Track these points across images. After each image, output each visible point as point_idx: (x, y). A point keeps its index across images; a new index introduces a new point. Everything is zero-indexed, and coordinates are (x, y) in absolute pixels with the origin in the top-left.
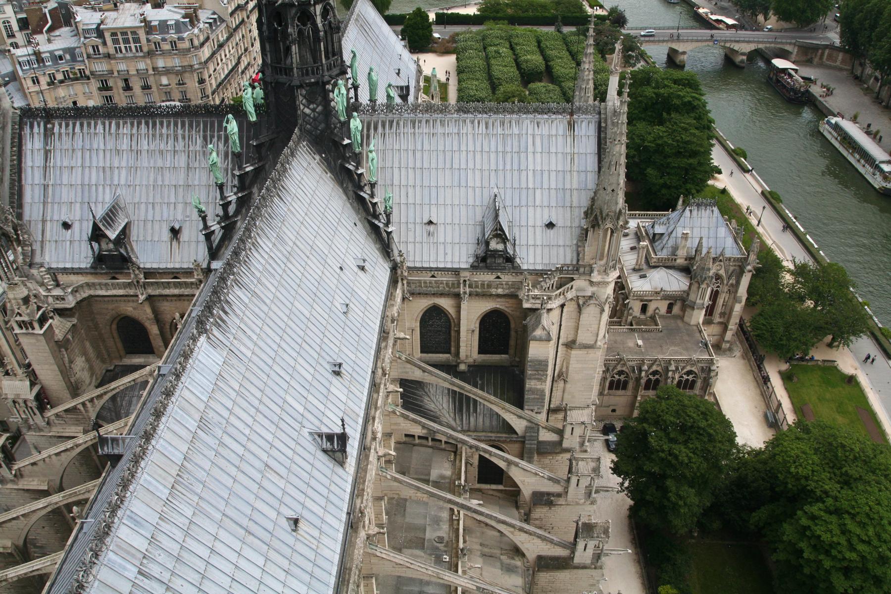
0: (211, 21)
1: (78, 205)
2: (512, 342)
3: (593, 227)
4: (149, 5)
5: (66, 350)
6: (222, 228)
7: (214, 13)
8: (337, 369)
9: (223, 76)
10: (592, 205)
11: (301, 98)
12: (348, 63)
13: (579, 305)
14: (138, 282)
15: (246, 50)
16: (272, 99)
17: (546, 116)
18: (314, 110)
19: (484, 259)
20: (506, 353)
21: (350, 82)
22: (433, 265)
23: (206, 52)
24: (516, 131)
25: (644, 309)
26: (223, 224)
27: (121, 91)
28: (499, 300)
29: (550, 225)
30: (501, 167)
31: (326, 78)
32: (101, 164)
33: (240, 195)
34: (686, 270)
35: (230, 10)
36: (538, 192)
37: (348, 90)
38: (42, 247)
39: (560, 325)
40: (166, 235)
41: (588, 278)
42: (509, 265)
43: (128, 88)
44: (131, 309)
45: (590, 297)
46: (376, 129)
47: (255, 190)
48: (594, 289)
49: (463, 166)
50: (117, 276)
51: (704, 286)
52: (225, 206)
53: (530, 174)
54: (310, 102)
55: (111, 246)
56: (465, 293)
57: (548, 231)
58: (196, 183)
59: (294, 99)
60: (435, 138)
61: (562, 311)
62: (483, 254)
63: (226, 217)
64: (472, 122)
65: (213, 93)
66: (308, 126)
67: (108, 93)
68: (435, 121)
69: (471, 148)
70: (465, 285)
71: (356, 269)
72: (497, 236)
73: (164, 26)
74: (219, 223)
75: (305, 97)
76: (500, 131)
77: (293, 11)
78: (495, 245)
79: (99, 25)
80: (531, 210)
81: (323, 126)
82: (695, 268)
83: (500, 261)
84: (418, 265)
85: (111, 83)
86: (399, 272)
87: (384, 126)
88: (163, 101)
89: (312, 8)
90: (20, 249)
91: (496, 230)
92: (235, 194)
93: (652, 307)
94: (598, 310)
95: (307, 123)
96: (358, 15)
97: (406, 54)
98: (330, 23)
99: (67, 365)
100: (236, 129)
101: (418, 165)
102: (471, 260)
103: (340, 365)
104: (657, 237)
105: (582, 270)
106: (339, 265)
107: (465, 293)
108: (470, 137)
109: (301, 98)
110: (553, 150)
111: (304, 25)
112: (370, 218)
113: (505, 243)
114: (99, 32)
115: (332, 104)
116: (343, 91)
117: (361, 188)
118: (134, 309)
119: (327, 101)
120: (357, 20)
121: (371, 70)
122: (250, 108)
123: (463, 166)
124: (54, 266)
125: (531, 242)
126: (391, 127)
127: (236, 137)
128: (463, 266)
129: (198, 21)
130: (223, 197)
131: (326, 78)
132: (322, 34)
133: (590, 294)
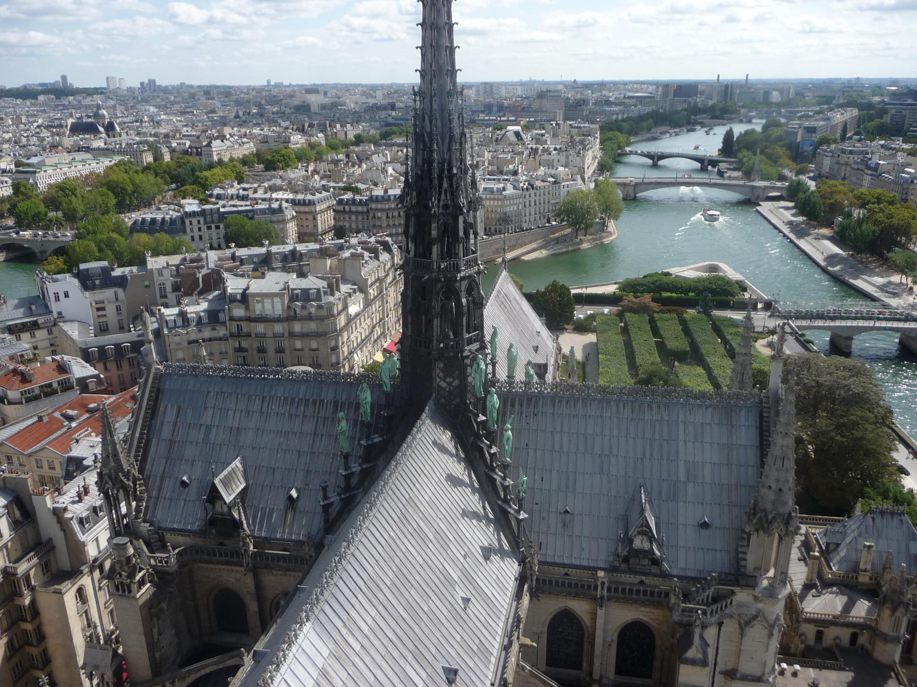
1: (200, 463)
2: (657, 664)
3: (757, 530)
4: (295, 276)
5: (159, 619)
6: (342, 500)
7: (354, 284)
8: (451, 677)
10: (756, 505)
11: (438, 371)
12: (488, 338)
13: (740, 625)
14: (245, 551)
18: (450, 384)
19: (626, 560)
20: (650, 677)
21: (489, 357)
22: (566, 561)
24: (666, 418)
25: (819, 636)
26: (343, 496)
27: (255, 352)
28: (642, 609)
29: (705, 525)
30: (648, 456)
31: (466, 353)
32: (229, 424)
33: (364, 466)
34: (872, 592)
35: (369, 282)
36: (690, 487)
37: (487, 365)
38: (156, 504)
39: (717, 648)
40: (281, 502)
41: (751, 591)
42: (655, 570)
43: (262, 350)
44: (233, 580)
45: (755, 617)
46: (513, 406)
47: (381, 463)
48: (760, 606)
49: (606, 452)
50: (227, 542)
51: (898, 614)
52: (348, 478)
53: (682, 464)
55: (225, 509)
56: (602, 597)
57: (703, 531)
58: (321, 450)
61: (720, 630)
62: (625, 553)
63: (347, 488)
64: (618, 406)
65: (344, 360)
66: (443, 400)
68: (576, 401)
69: (616, 433)
70: (603, 588)
71: (482, 560)
72: (639, 533)
73: (306, 292)
74: (339, 495)
75: (442, 370)
76: (647, 416)
78: (639, 543)
79: (245, 290)
80: (681, 504)
81: (458, 400)
82: (884, 589)
83: (646, 562)
84: (549, 559)
86: (528, 566)
88: (295, 365)
89: (457, 284)
90: (134, 504)
91: (642, 526)
92: (360, 465)
93: (831, 633)
94: (766, 632)
96: (499, 291)
97: (545, 332)
98: (474, 298)
99: (156, 637)
100: (369, 399)
101: (557, 448)
102: (611, 559)
103: (456, 672)
104: (832, 547)
105: (743, 582)
106: (463, 553)
107: (602, 597)
109: (438, 371)
110: (707, 439)
111: (449, 299)
112: (500, 502)
113: (651, 543)
114: (245, 298)
115: (470, 379)
116: (483, 366)
117: (492, 469)
118: (237, 580)
119: (463, 376)
120: (497, 296)
121: (511, 346)
123: (606, 452)
124: (163, 525)
125: (681, 543)
126: (529, 405)
128: (601, 565)
130: (347, 468)
131: (466, 353)
133: (754, 613)
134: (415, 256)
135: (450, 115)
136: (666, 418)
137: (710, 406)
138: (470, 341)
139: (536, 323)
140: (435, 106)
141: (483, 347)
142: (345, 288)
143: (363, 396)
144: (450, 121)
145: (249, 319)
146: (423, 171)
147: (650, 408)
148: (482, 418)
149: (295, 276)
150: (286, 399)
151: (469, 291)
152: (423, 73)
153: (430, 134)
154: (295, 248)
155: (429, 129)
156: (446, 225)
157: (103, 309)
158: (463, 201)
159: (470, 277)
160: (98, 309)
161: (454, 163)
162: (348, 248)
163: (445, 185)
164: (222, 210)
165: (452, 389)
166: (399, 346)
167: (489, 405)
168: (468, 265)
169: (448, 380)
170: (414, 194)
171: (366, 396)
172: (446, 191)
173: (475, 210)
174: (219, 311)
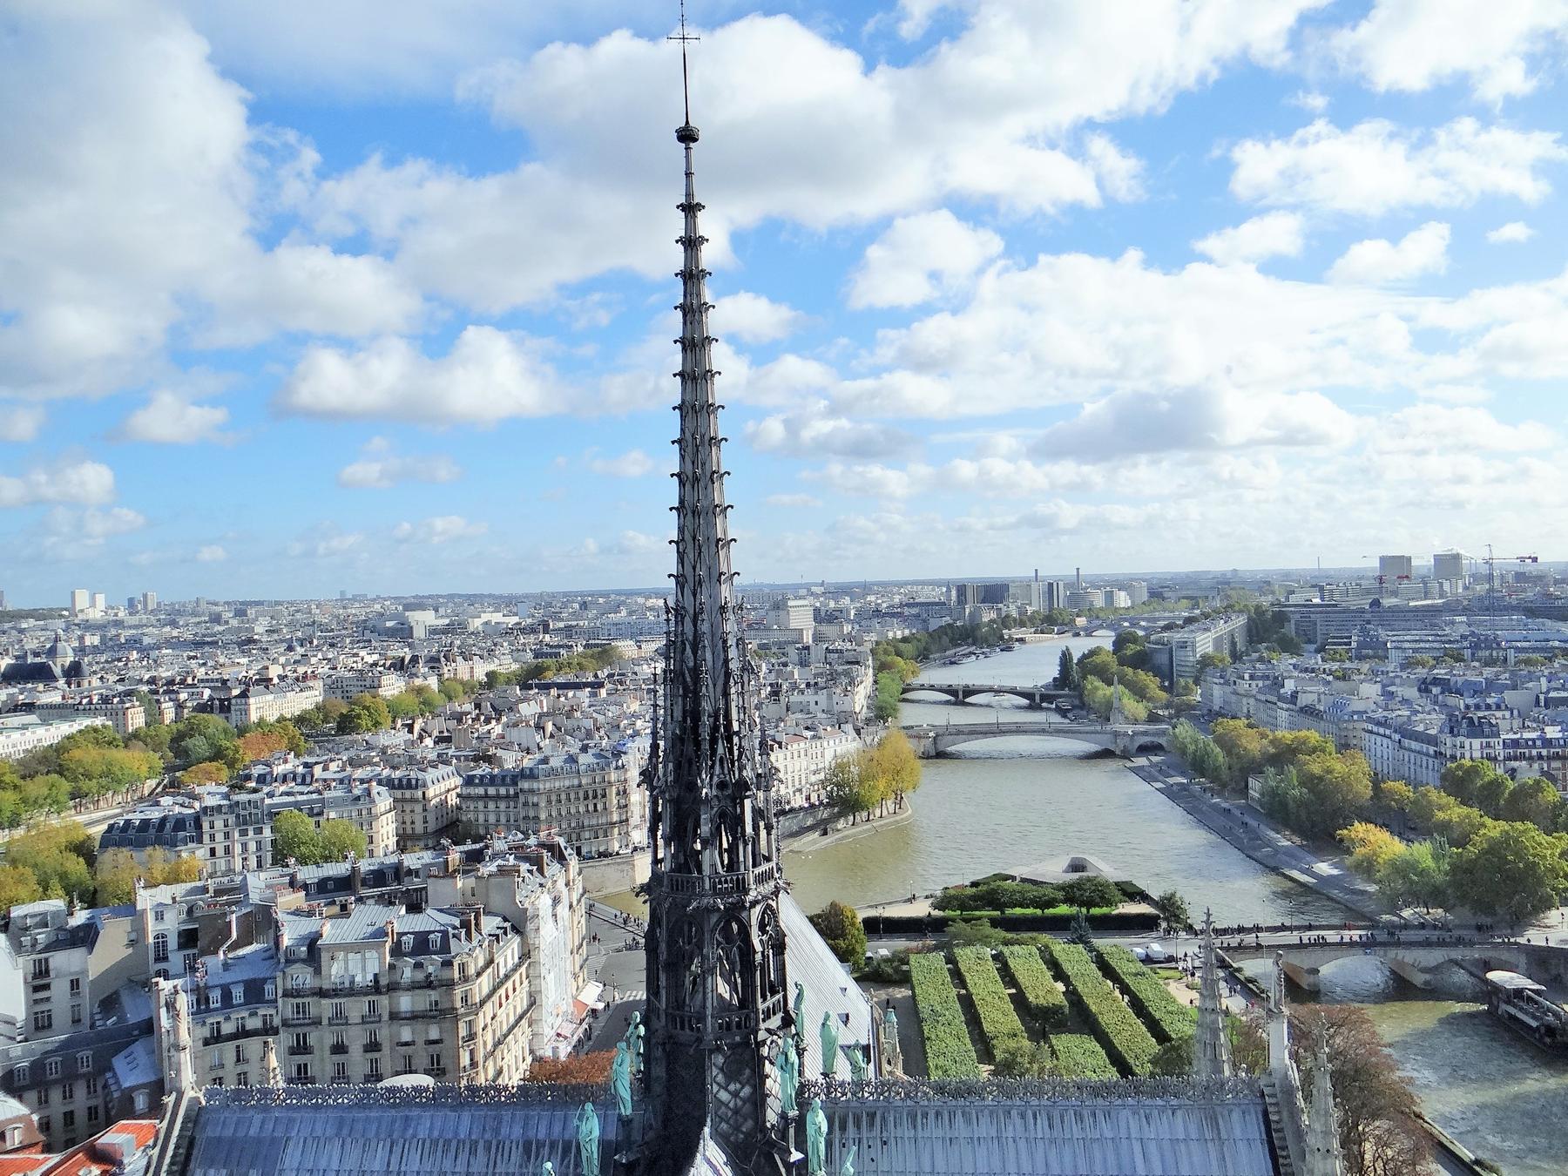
0: (500, 932)
7: (505, 920)
9: (505, 1029)
12: (791, 1004)
16: (659, 1071)
17: (1159, 1102)
18: (735, 1094)
23: (484, 984)
27: (327, 1052)
43: (340, 1049)
46: (843, 1128)
54: (731, 1076)
59: (701, 1070)
60: (956, 1147)
64: (1023, 1116)
66: (724, 1126)
68: (952, 1115)
75: (722, 1069)
76: (1077, 1133)
77: (714, 919)
85: (311, 1040)
87: (858, 1126)
88: (397, 1074)
89: (744, 914)
95: (722, 1119)
100: (596, 1133)
108: (1022, 1144)
115: (769, 1082)
122: (625, 1092)
126: (871, 1124)
127: (595, 1149)
129: (478, 930)
131: (762, 1035)
132: (758, 957)
134: (672, 870)
135: (725, 642)
136: (1108, 1134)
137: (1180, 1107)
139: (839, 974)
140: (705, 627)
141: (788, 1021)
142: (489, 924)
143: (584, 1128)
144: (725, 649)
145: (321, 993)
146: (683, 730)
147: (1079, 1117)
148: (796, 1156)
149: (403, 911)
150: (435, 1143)
151: (762, 928)
152: (680, 579)
153: (696, 671)
154: (400, 863)
155: (691, 664)
156: (722, 815)
157: (47, 987)
158: (748, 774)
159: (765, 898)
160: (36, 989)
161: (734, 716)
162: (494, 857)
163: (720, 750)
164: (268, 801)
165: (740, 1103)
166: (642, 1030)
167: (810, 1130)
168: (762, 879)
169: (732, 1087)
170: (671, 765)
171: (591, 1128)
172: (721, 760)
173: (767, 789)
174: (264, 981)
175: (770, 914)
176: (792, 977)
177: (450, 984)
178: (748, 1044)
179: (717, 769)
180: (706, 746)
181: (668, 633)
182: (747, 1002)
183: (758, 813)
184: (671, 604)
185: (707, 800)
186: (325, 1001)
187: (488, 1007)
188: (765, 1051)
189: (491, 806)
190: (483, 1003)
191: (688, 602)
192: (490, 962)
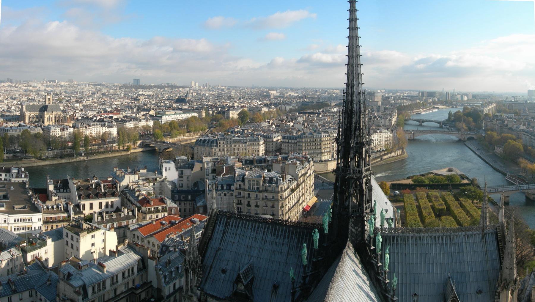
12: (373, 206)
15: (303, 194)
23: (286, 193)
27: (246, 206)
65: (286, 213)
67: (240, 206)
85: (242, 202)
88: (263, 214)
126: (393, 241)
129: (286, 179)
131: (364, 214)
132: (365, 192)
138: (366, 209)
140: (355, 98)
141: (372, 211)
144: (360, 104)
146: (347, 127)
149: (266, 171)
151: (366, 184)
153: (351, 111)
156: (357, 152)
158: (364, 140)
159: (367, 176)
161: (361, 124)
163: (357, 133)
173: (369, 145)
175: (368, 182)
176: (373, 199)
177: (278, 192)
178: (360, 216)
179: (356, 139)
180: (353, 132)
181: (344, 100)
182: (361, 205)
183: (366, 152)
184: (345, 91)
185: (353, 147)
186: (246, 192)
187: (287, 200)
188: (365, 218)
189: (290, 145)
190: (286, 198)
191: (350, 91)
192: (288, 188)
